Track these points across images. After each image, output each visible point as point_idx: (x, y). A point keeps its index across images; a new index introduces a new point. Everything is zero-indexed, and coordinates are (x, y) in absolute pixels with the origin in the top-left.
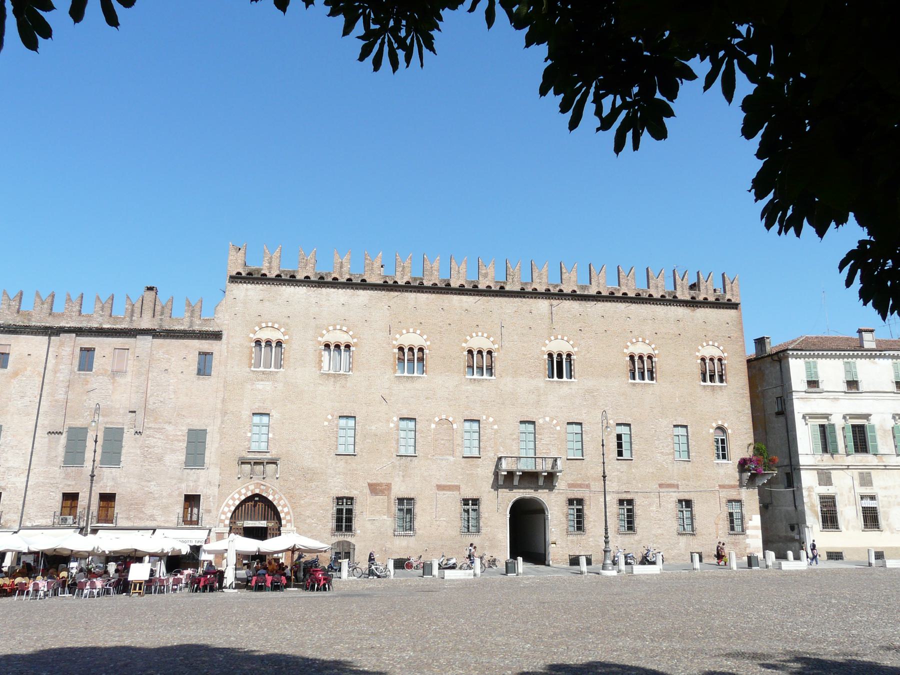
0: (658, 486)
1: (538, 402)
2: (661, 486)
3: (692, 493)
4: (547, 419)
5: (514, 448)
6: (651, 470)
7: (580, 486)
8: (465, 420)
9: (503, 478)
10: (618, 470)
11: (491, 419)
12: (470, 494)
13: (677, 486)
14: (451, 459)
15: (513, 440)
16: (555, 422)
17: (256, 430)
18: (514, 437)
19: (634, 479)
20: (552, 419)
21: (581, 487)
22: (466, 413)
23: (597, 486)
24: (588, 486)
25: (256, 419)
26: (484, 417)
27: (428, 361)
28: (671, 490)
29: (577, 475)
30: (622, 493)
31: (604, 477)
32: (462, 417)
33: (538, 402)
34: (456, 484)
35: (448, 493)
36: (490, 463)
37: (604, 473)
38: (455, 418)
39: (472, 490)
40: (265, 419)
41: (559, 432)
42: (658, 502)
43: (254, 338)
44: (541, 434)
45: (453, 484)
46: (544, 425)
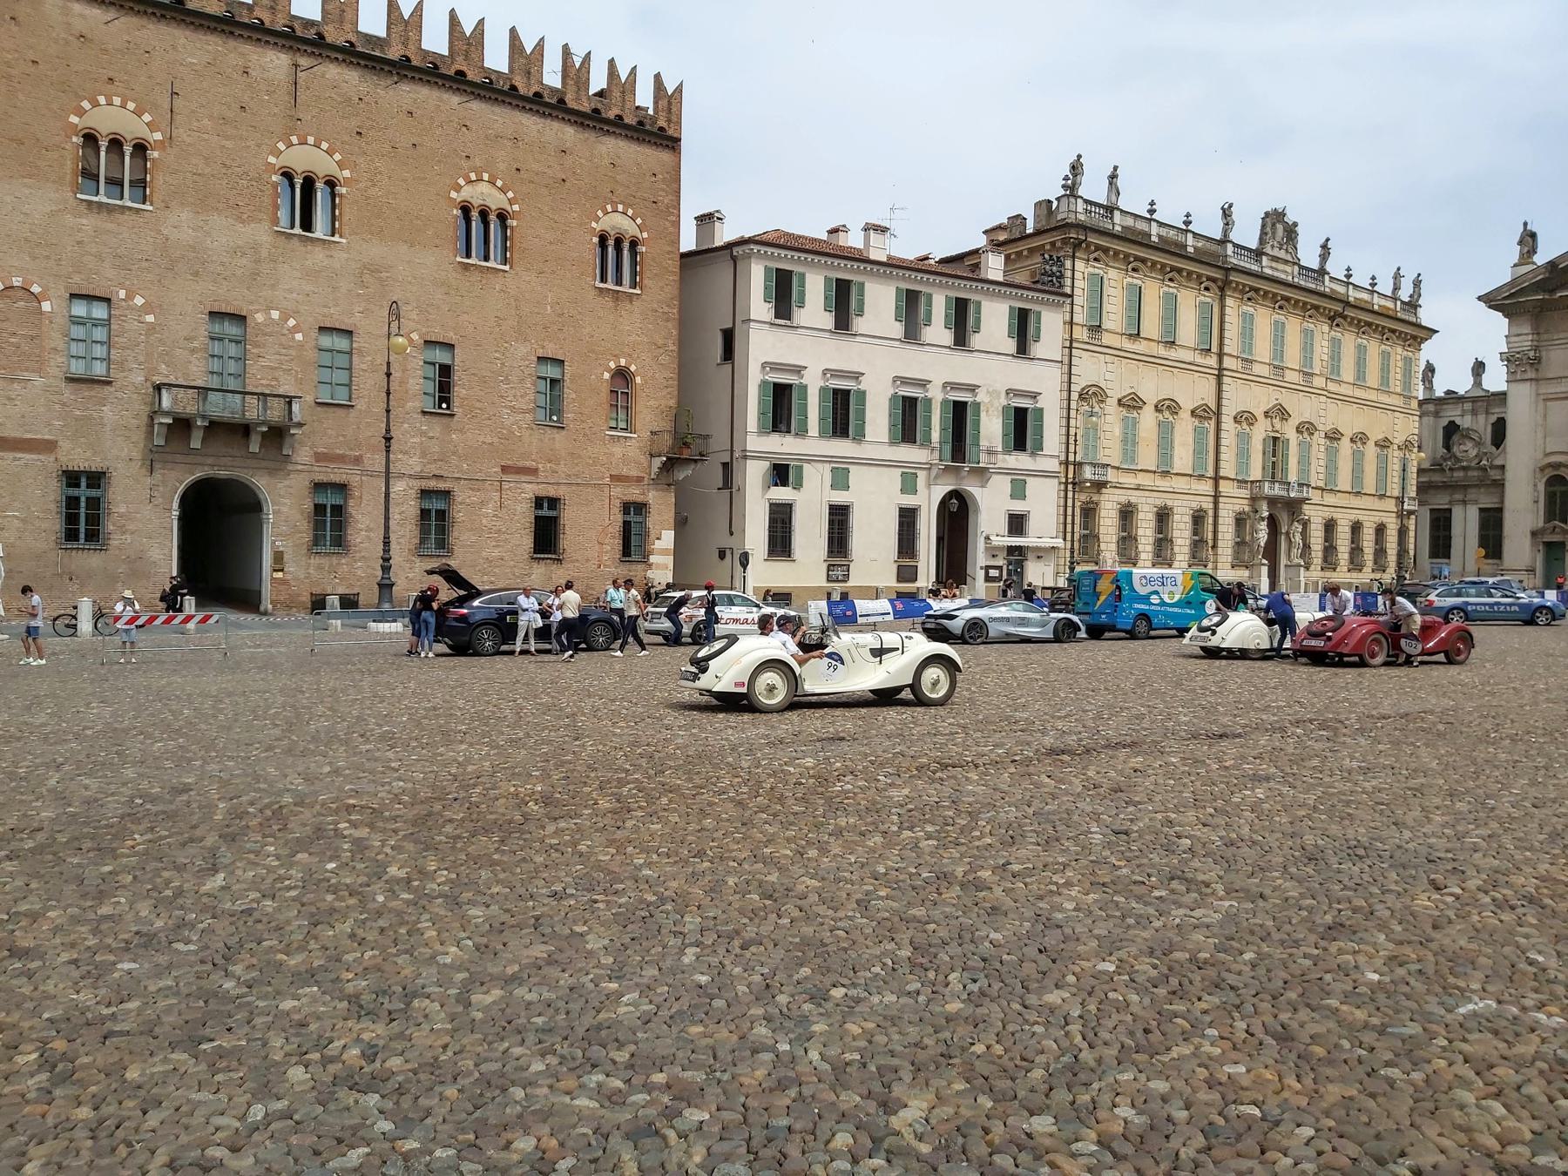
0: (498, 469)
1: (255, 275)
2: (505, 469)
3: (563, 488)
4: (275, 315)
5: (195, 369)
6: (489, 440)
7: (341, 459)
8: (73, 296)
9: (165, 430)
10: (423, 434)
11: (139, 301)
12: (80, 459)
13: (533, 471)
14: (39, 381)
15: (193, 351)
16: (292, 322)
17: (79, 332)
18: (196, 344)
19: (454, 453)
20: (285, 317)
21: (345, 462)
22: (77, 279)
23: (376, 461)
24: (358, 460)
25: (80, 309)
26: (122, 294)
27: (159, 182)
28: (524, 478)
29: (338, 436)
30: (428, 478)
31: (388, 439)
32: (66, 287)
33: (255, 275)
34: (46, 437)
35: (27, 456)
36: (135, 396)
37: (388, 430)
38: (45, 289)
39: (88, 454)
40: (99, 311)
41: (301, 345)
42: (497, 498)
43: (459, 200)
44: (259, 346)
45: (39, 437)
46: (266, 325)
